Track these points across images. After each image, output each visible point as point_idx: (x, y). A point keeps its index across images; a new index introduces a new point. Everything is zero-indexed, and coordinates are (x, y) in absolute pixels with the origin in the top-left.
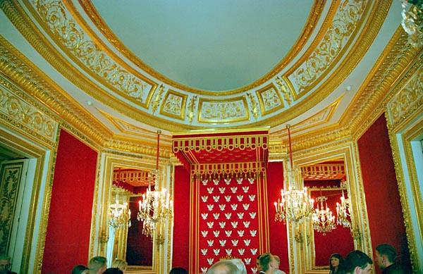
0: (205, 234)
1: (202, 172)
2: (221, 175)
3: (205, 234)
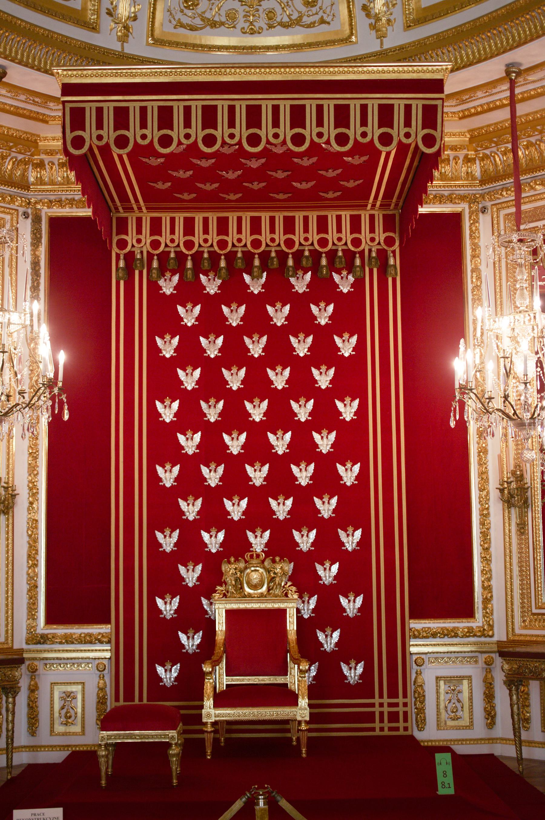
0: (168, 476)
1: (155, 244)
2: (231, 257)
3: (168, 476)
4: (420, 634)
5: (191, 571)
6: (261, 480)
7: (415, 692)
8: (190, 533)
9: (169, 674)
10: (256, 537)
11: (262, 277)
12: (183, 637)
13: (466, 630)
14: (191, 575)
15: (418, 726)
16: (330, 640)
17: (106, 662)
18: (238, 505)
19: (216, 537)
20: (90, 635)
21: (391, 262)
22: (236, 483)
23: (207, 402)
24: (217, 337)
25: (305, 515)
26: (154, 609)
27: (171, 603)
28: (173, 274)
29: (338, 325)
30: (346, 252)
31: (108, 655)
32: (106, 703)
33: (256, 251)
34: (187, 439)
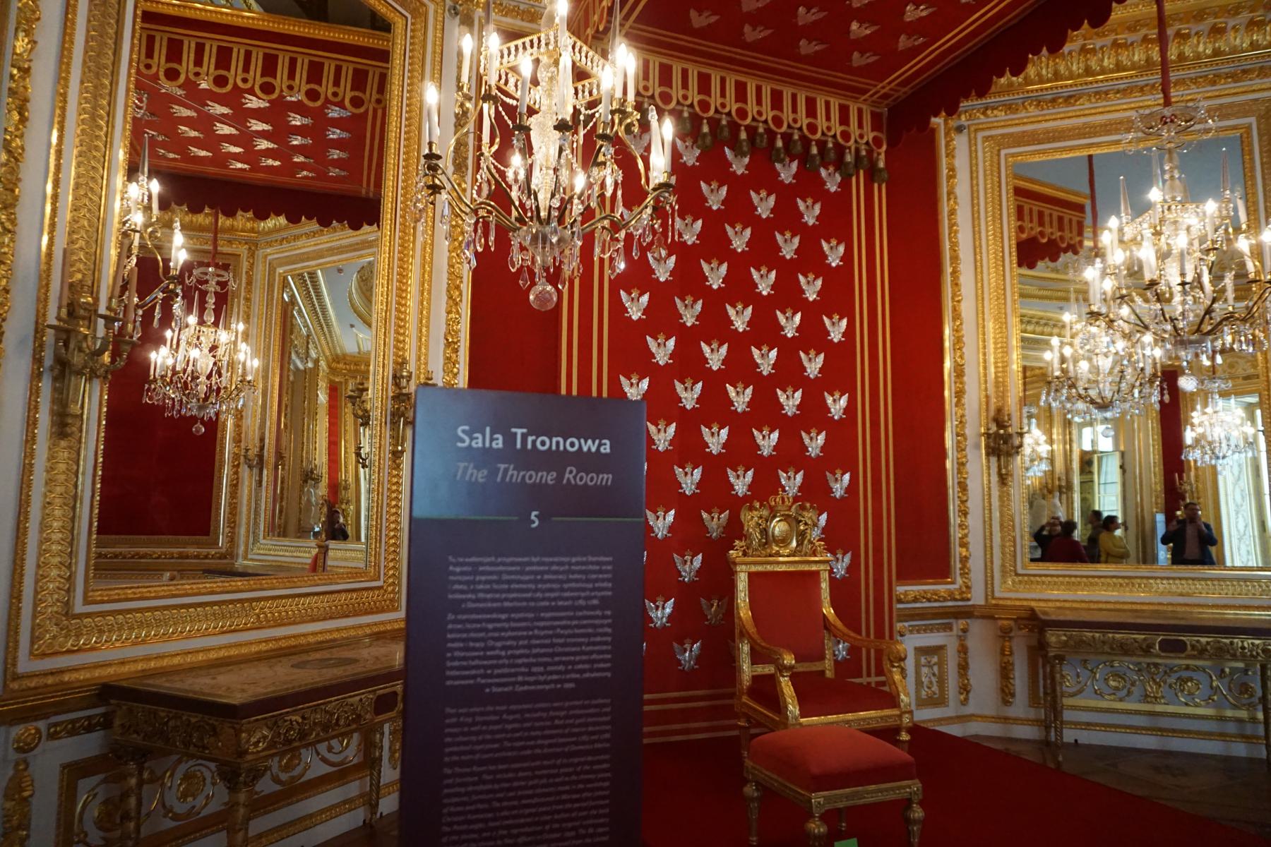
0: (636, 389)
2: (714, 123)
22: (714, 407)
23: (683, 300)
30: (836, 144)
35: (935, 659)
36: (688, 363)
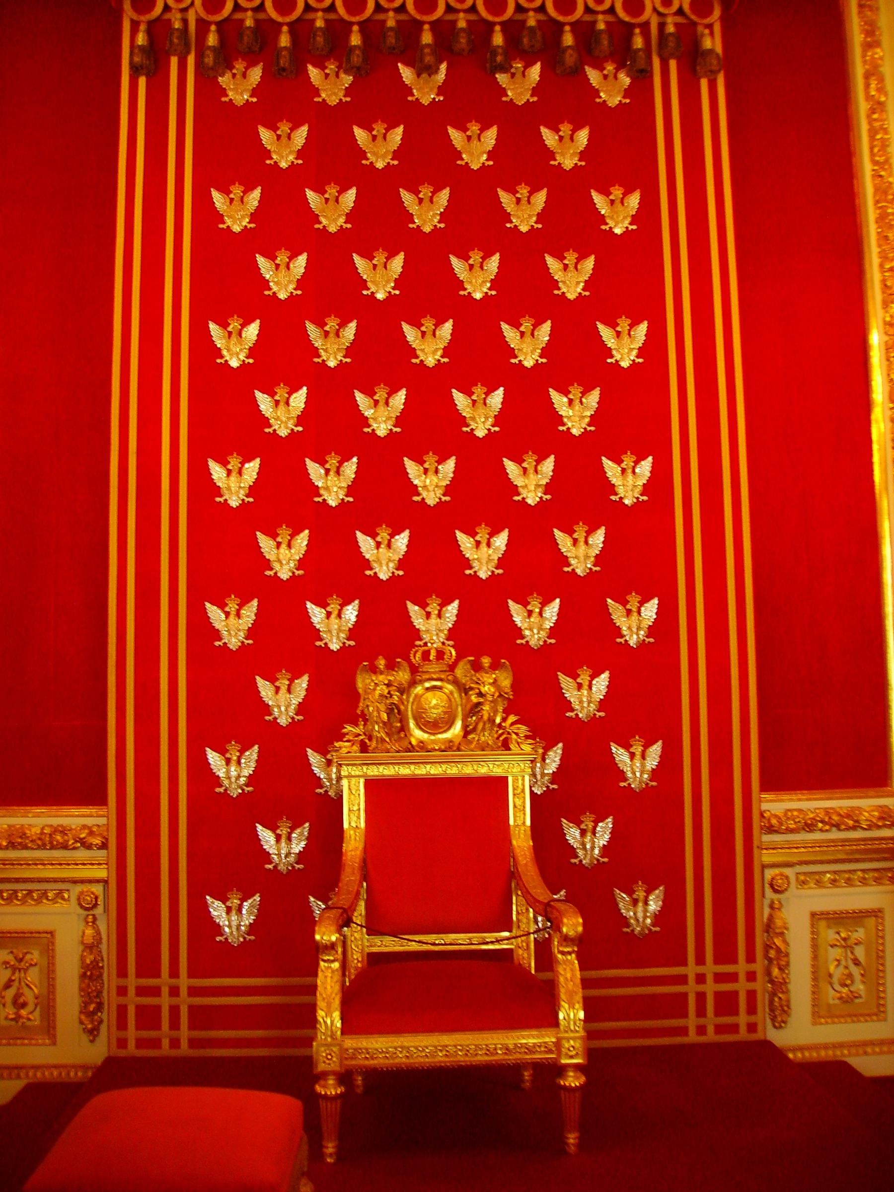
2: (371, 29)
4: (781, 824)
5: (284, 689)
6: (439, 492)
7: (767, 947)
8: (284, 611)
9: (234, 918)
10: (428, 615)
11: (437, 70)
12: (266, 837)
13: (876, 814)
14: (283, 699)
15: (774, 1019)
16: (590, 840)
17: (98, 889)
18: (389, 546)
19: (339, 616)
20: (63, 831)
21: (707, 44)
22: (382, 499)
23: (321, 324)
24: (343, 190)
25: (533, 570)
26: (202, 774)
27: (239, 762)
28: (251, 64)
29: (600, 169)
31: (102, 874)
32: (101, 975)
33: (426, 18)
34: (277, 403)
35: (860, 934)
36: (332, 427)
